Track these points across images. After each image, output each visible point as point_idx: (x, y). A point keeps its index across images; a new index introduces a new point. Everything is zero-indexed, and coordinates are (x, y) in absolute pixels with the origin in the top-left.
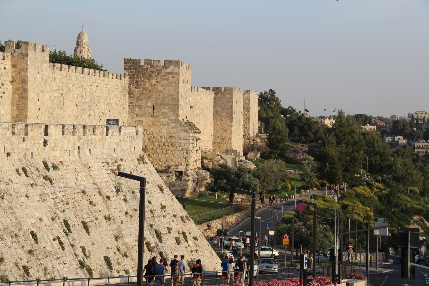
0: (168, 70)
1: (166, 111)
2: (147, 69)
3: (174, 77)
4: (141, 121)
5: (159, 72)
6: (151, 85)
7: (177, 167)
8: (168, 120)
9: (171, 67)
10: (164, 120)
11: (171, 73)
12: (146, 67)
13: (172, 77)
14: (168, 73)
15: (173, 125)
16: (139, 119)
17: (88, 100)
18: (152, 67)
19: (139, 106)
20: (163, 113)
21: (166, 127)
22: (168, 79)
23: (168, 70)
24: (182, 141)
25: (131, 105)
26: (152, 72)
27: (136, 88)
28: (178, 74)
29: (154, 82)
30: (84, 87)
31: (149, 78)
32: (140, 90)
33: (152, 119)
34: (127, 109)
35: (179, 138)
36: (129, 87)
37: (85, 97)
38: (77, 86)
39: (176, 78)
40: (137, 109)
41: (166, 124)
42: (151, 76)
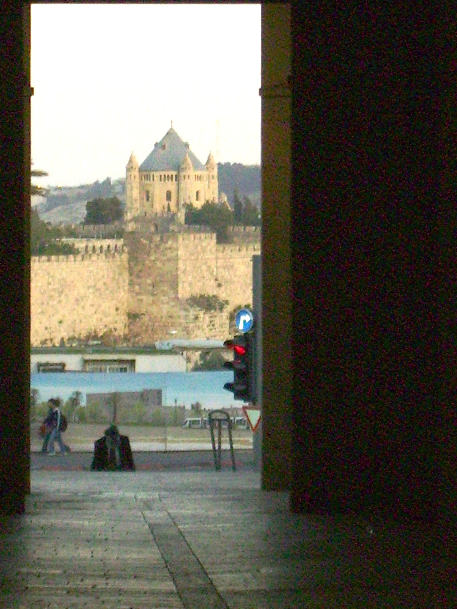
0: (168, 246)
1: (166, 288)
3: (172, 252)
4: (141, 300)
5: (157, 247)
6: (150, 261)
9: (170, 242)
10: (163, 298)
11: (170, 248)
14: (166, 249)
15: (173, 304)
16: (140, 297)
17: (56, 286)
18: (151, 242)
19: (139, 285)
20: (163, 291)
21: (166, 306)
23: (168, 246)
25: (131, 284)
27: (136, 265)
28: (177, 249)
29: (152, 258)
30: (52, 274)
31: (149, 254)
32: (140, 267)
33: (151, 298)
34: (126, 288)
35: (179, 317)
36: (129, 264)
37: (52, 283)
38: (41, 275)
39: (174, 254)
40: (137, 287)
42: (149, 252)
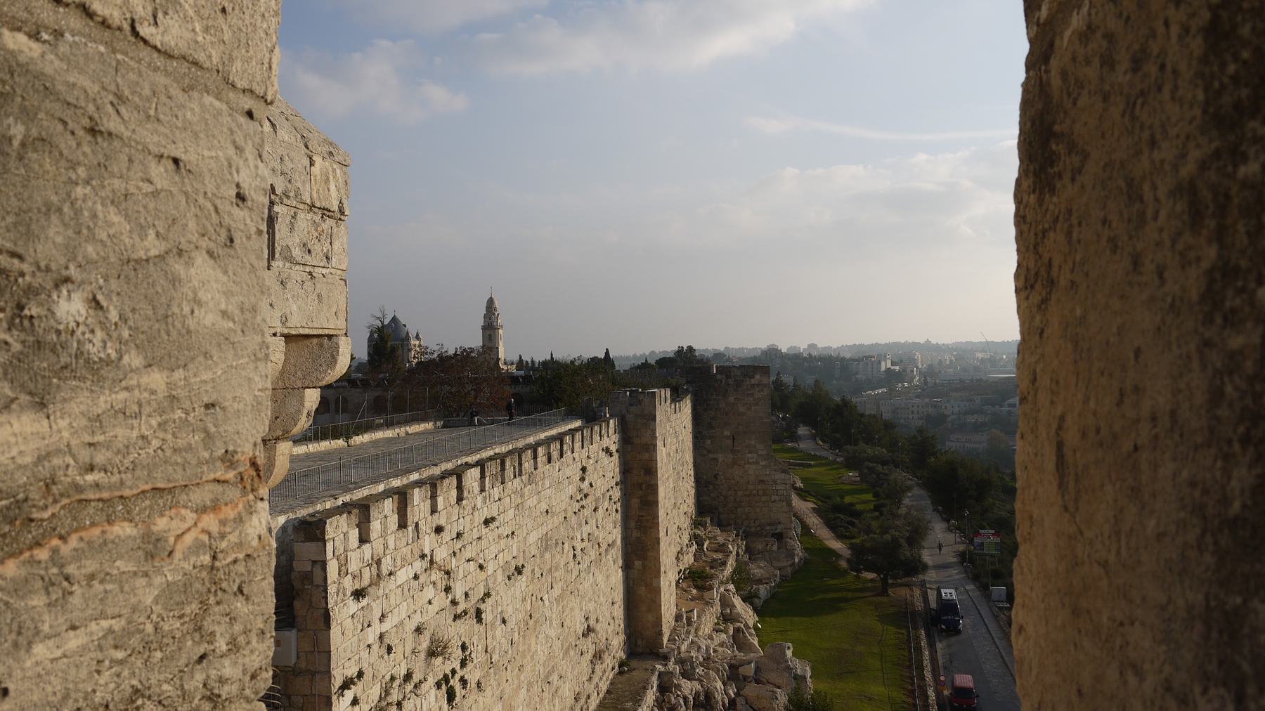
1: (753, 442)
2: (721, 381)
7: (774, 527)
8: (755, 455)
9: (757, 377)
11: (758, 385)
12: (719, 377)
13: (759, 391)
14: (753, 385)
16: (711, 456)
18: (728, 377)
22: (753, 394)
23: (753, 381)
24: (779, 487)
26: (728, 385)
29: (731, 399)
33: (731, 456)
35: (775, 482)
41: (754, 463)
